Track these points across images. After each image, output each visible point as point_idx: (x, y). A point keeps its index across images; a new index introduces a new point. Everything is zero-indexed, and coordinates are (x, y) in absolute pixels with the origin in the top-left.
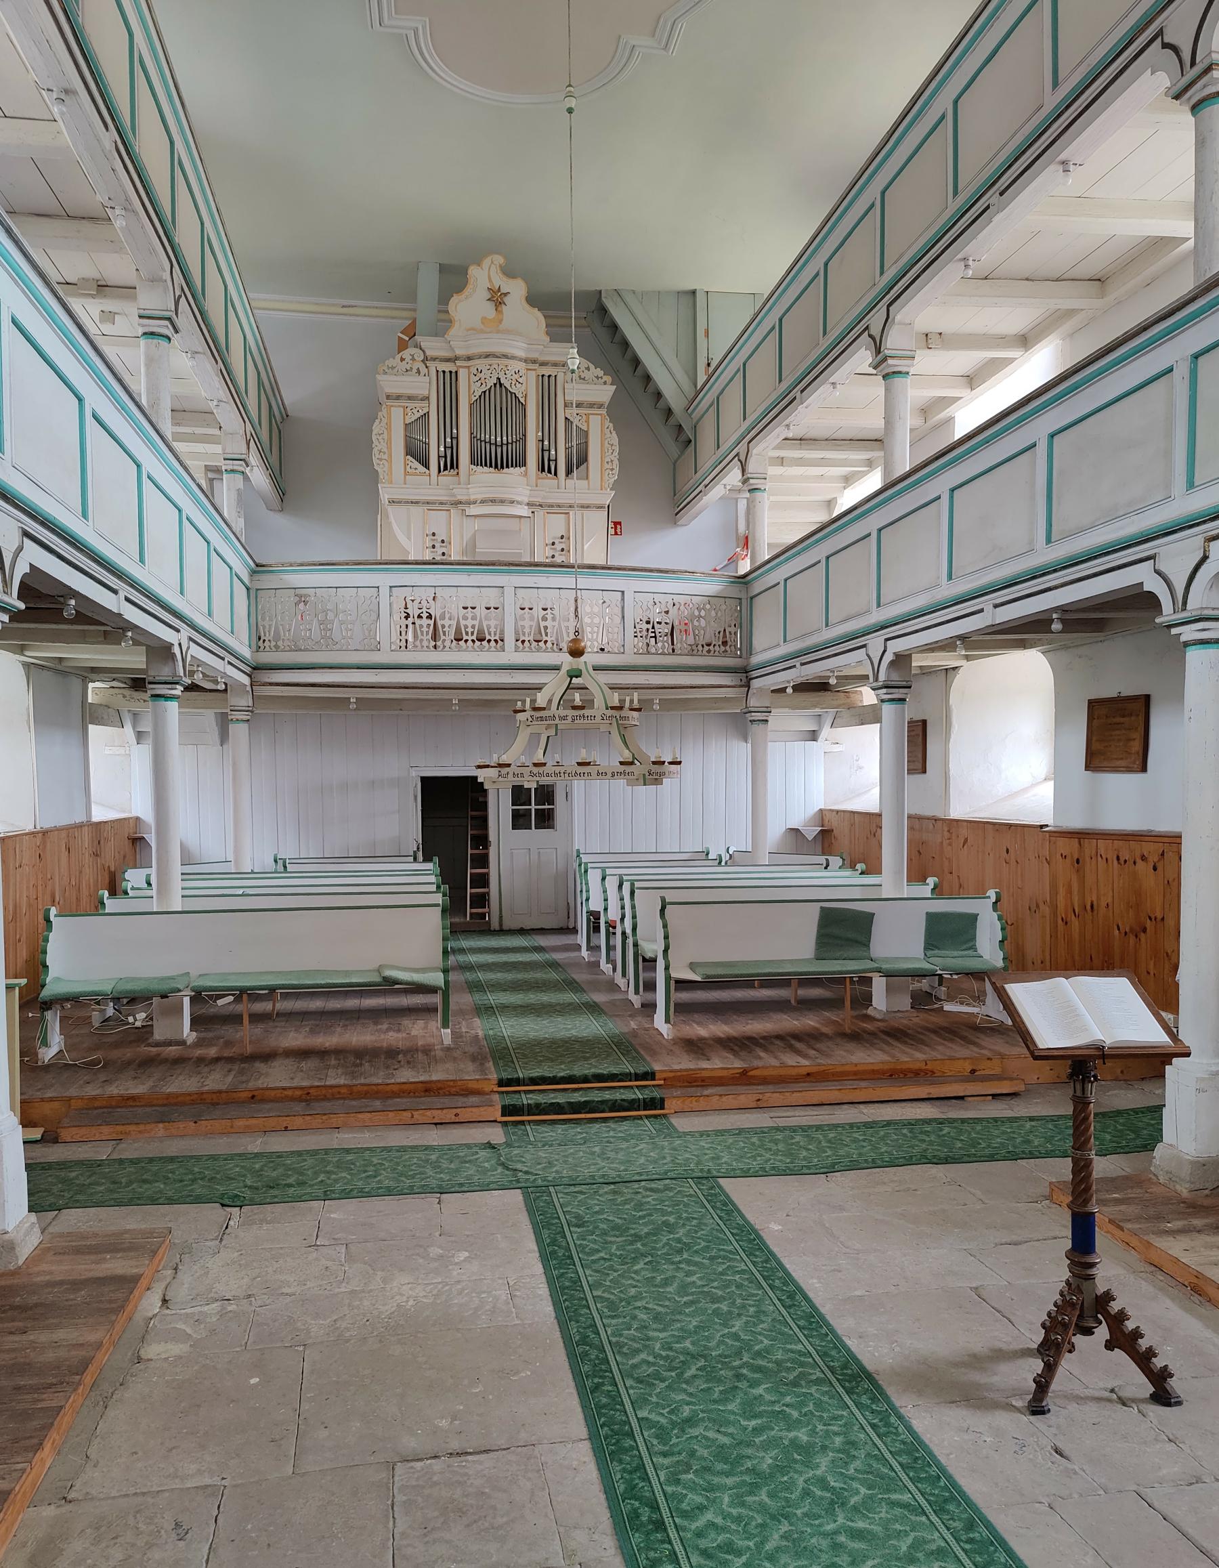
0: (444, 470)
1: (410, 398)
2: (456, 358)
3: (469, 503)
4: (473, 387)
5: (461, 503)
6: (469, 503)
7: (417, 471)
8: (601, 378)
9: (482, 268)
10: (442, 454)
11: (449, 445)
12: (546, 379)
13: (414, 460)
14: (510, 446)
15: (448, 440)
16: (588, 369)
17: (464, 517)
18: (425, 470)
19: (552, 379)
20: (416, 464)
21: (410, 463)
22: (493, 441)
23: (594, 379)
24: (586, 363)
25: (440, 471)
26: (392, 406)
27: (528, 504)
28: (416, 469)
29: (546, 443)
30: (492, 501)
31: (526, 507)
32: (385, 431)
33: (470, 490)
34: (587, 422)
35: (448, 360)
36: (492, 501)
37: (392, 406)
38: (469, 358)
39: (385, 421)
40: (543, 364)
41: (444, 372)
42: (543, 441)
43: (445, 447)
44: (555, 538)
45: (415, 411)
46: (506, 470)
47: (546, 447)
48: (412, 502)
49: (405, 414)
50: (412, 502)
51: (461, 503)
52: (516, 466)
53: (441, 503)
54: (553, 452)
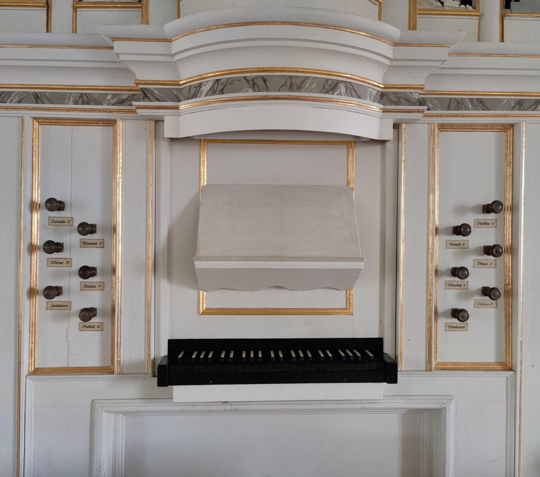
5: (146, 94)
17: (164, 145)
30: (253, 84)
31: (376, 107)
33: (177, 46)
36: (253, 84)
44: (462, 209)
51: (146, 94)
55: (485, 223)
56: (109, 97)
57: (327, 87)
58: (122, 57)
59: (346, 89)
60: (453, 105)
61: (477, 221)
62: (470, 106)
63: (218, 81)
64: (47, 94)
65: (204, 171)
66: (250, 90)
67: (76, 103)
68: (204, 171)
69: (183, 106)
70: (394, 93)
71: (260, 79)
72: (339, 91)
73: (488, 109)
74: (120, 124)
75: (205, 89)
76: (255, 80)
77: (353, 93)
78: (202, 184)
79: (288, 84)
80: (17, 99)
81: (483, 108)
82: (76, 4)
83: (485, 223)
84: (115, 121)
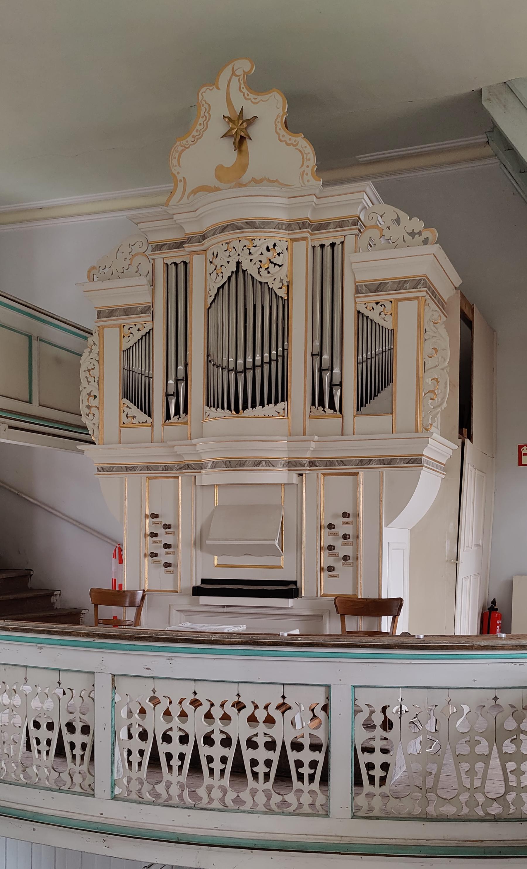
0: (175, 415)
1: (127, 311)
2: (189, 240)
3: (201, 466)
4: (210, 283)
6: (201, 466)
7: (135, 421)
8: (420, 233)
9: (218, 88)
10: (172, 390)
11: (181, 375)
12: (328, 250)
13: (131, 405)
14: (258, 371)
15: (181, 367)
16: (398, 221)
18: (145, 417)
19: (338, 249)
20: (134, 410)
21: (127, 410)
22: (231, 366)
23: (408, 238)
24: (391, 212)
25: (168, 417)
26: (104, 327)
27: (291, 464)
28: (134, 417)
29: (326, 357)
32: (96, 363)
34: (394, 314)
35: (179, 245)
37: (104, 327)
38: (204, 237)
39: (96, 349)
40: (322, 226)
41: (176, 264)
42: (321, 354)
43: (177, 381)
45: (134, 330)
46: (249, 411)
47: (326, 364)
48: (127, 469)
49: (122, 337)
50: (127, 469)
52: (269, 402)
53: (166, 468)
54: (336, 371)
55: (347, 523)
56: (176, 466)
57: (256, 463)
58: (178, 453)
59: (266, 463)
60: (328, 464)
61: (343, 522)
62: (337, 464)
63: (213, 462)
64: (152, 466)
65: (216, 498)
66: (225, 466)
67: (163, 470)
68: (216, 498)
69: (203, 471)
70: (294, 461)
71: (228, 462)
72: (262, 464)
73: (346, 466)
74: (180, 478)
75: (210, 465)
76: (226, 462)
77: (270, 464)
78: (216, 505)
79: (239, 463)
80: (140, 469)
81: (343, 464)
82: (163, 424)
83: (347, 523)
84: (178, 476)
